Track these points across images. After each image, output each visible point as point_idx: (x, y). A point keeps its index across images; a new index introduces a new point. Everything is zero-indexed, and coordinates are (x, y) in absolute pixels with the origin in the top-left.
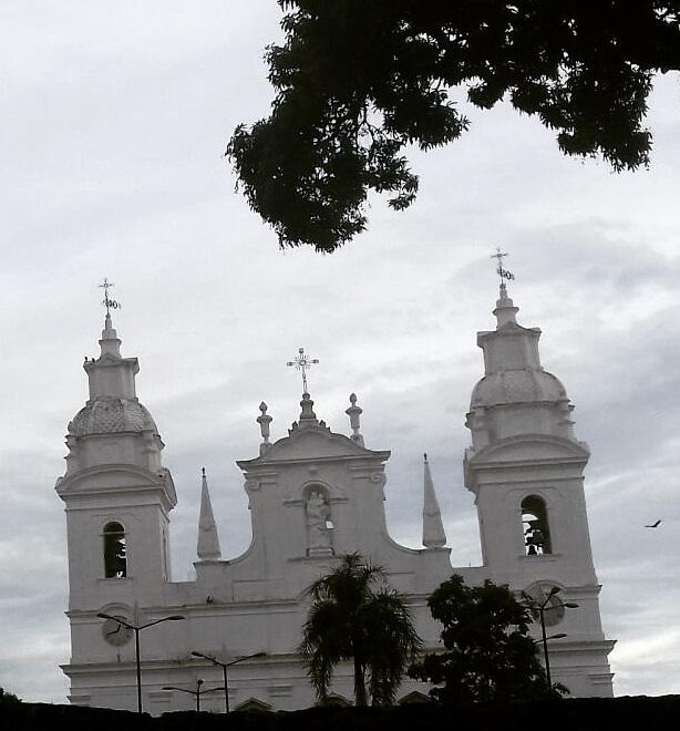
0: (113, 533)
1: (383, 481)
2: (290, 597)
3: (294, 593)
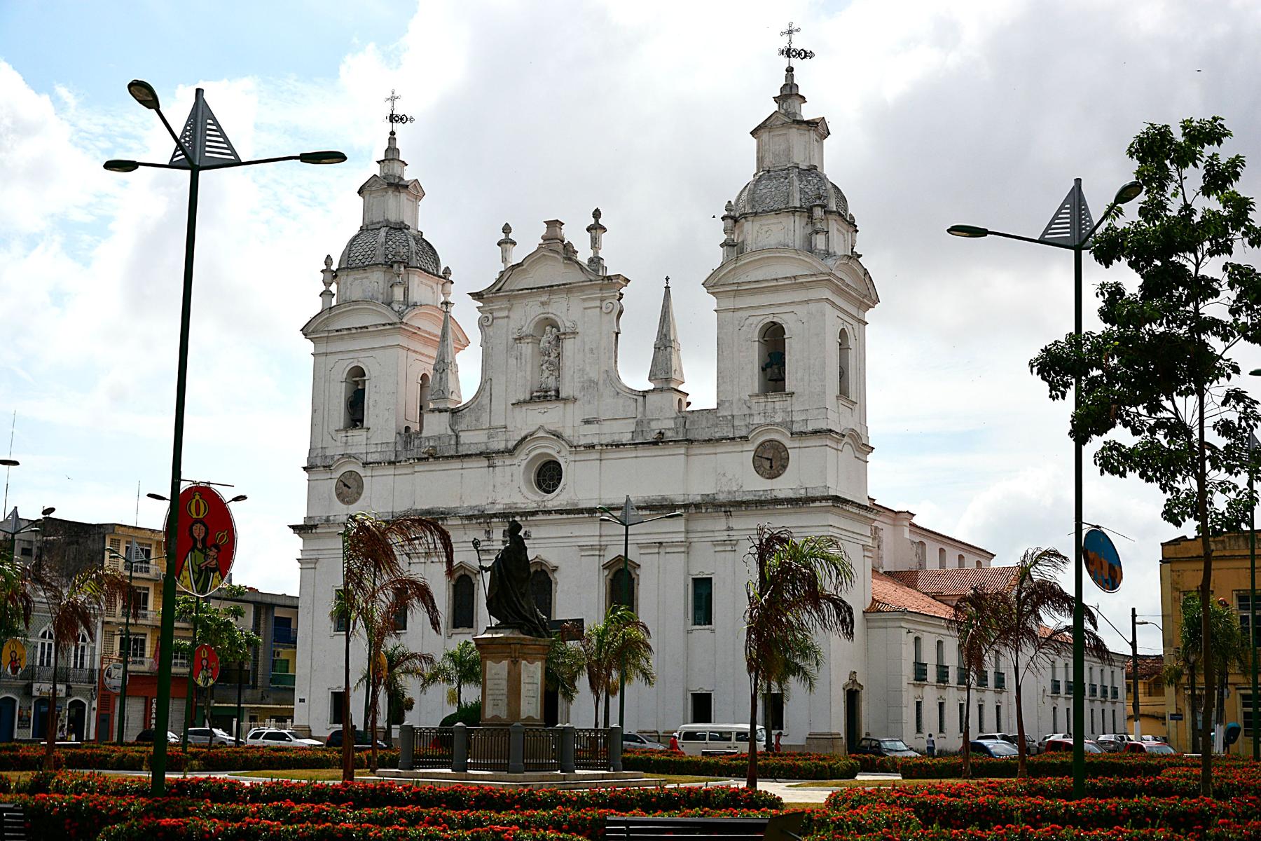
0: (774, 339)
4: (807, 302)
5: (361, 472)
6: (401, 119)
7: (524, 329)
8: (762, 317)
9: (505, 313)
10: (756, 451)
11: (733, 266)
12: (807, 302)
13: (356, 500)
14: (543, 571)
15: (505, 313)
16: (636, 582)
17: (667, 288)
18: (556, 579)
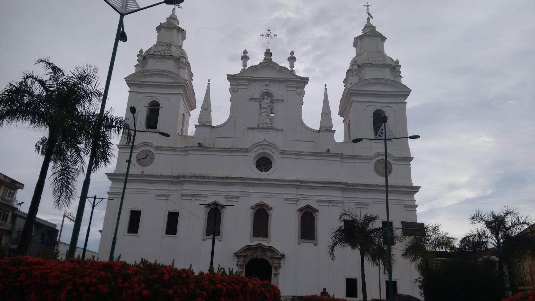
1: (302, 94)
2: (246, 147)
3: (248, 146)
4: (397, 103)
5: (154, 151)
10: (375, 164)
12: (397, 103)
13: (148, 165)
14: (264, 209)
16: (315, 218)
17: (326, 89)
18: (270, 213)
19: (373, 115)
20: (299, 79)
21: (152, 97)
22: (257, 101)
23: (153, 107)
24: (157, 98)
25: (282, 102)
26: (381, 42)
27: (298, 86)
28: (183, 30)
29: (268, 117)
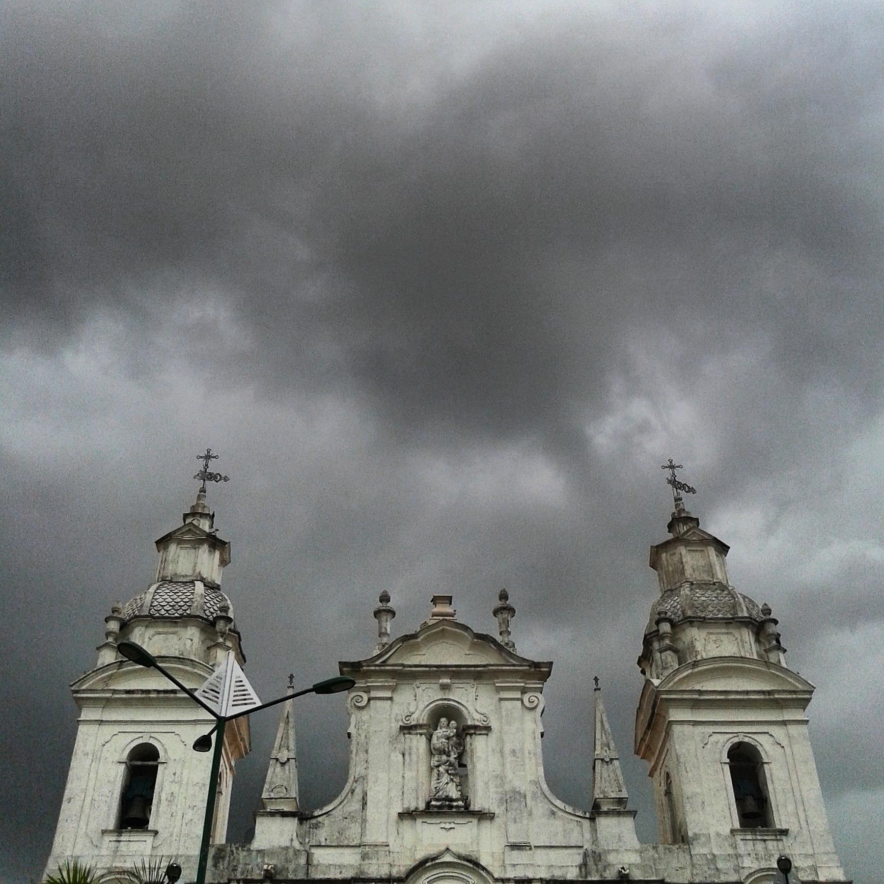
6: (212, 477)
7: (415, 716)
8: (732, 735)
9: (388, 694)
11: (690, 671)
15: (388, 694)
19: (728, 761)
20: (527, 668)
21: (140, 735)
22: (421, 734)
23: (139, 763)
24: (152, 735)
25: (487, 735)
26: (717, 556)
27: (527, 686)
28: (224, 543)
29: (452, 780)
